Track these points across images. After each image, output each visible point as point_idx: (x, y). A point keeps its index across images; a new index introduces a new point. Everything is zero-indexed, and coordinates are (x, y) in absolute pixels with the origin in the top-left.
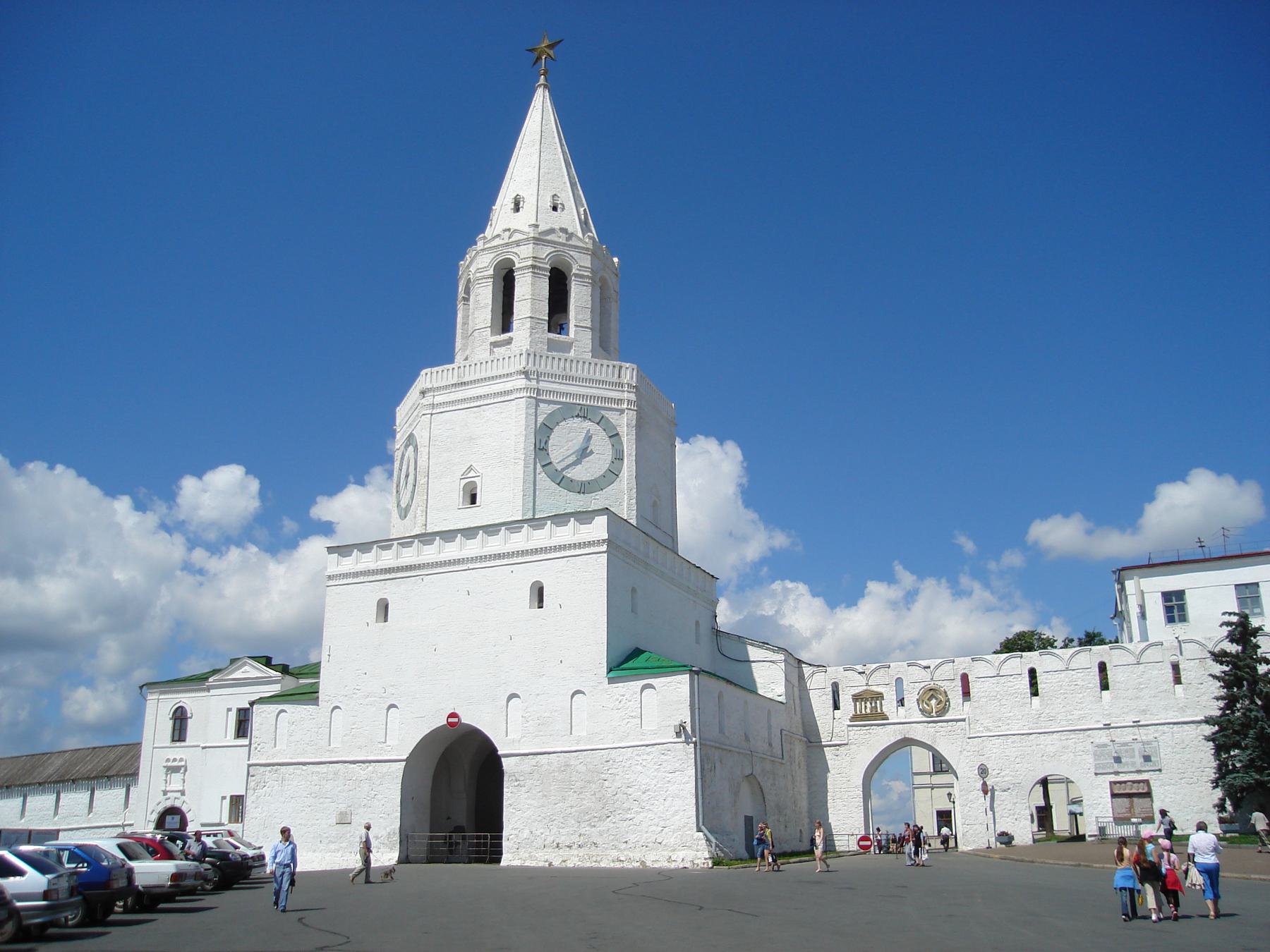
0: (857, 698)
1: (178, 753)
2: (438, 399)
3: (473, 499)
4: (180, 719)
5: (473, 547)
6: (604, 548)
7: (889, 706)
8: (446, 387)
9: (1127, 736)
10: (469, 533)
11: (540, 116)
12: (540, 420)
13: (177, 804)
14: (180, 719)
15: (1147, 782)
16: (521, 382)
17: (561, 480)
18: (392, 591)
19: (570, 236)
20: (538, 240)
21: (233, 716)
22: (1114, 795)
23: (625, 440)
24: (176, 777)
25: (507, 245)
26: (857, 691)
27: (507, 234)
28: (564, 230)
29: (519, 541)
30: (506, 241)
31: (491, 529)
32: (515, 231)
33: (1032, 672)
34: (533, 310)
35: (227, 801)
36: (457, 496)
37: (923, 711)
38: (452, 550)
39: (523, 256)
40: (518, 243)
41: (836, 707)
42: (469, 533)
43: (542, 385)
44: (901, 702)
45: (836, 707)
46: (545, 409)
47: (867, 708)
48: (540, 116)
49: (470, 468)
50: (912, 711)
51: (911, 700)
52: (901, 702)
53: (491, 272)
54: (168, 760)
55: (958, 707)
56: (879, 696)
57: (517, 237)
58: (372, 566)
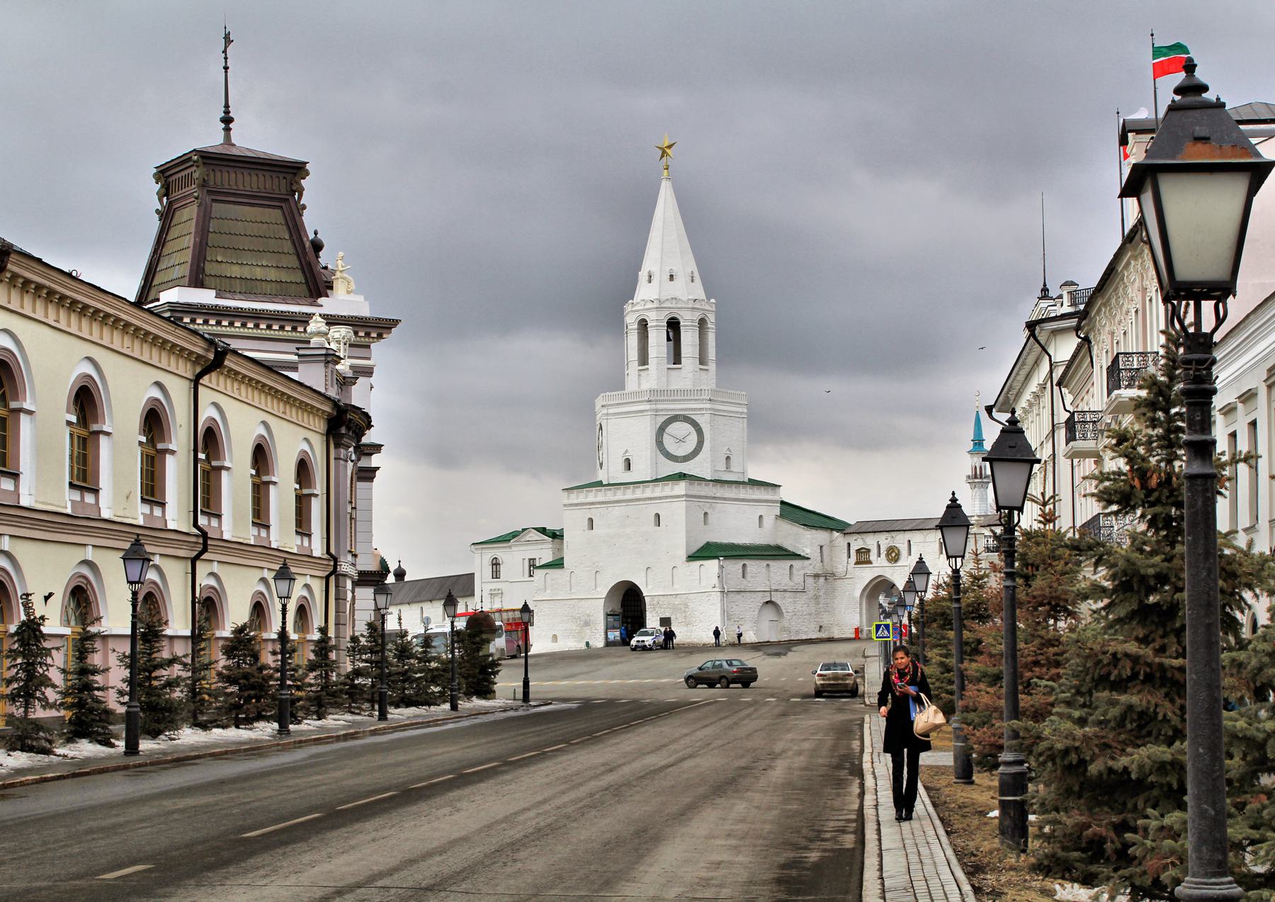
0: (858, 551)
1: (496, 585)
2: (611, 411)
4: (496, 564)
5: (629, 494)
7: (873, 556)
14: (496, 564)
17: (669, 456)
18: (595, 513)
24: (497, 599)
29: (648, 492)
36: (621, 465)
38: (620, 495)
39: (652, 317)
43: (660, 406)
45: (849, 557)
46: (661, 420)
51: (883, 556)
56: (869, 551)
57: (649, 305)
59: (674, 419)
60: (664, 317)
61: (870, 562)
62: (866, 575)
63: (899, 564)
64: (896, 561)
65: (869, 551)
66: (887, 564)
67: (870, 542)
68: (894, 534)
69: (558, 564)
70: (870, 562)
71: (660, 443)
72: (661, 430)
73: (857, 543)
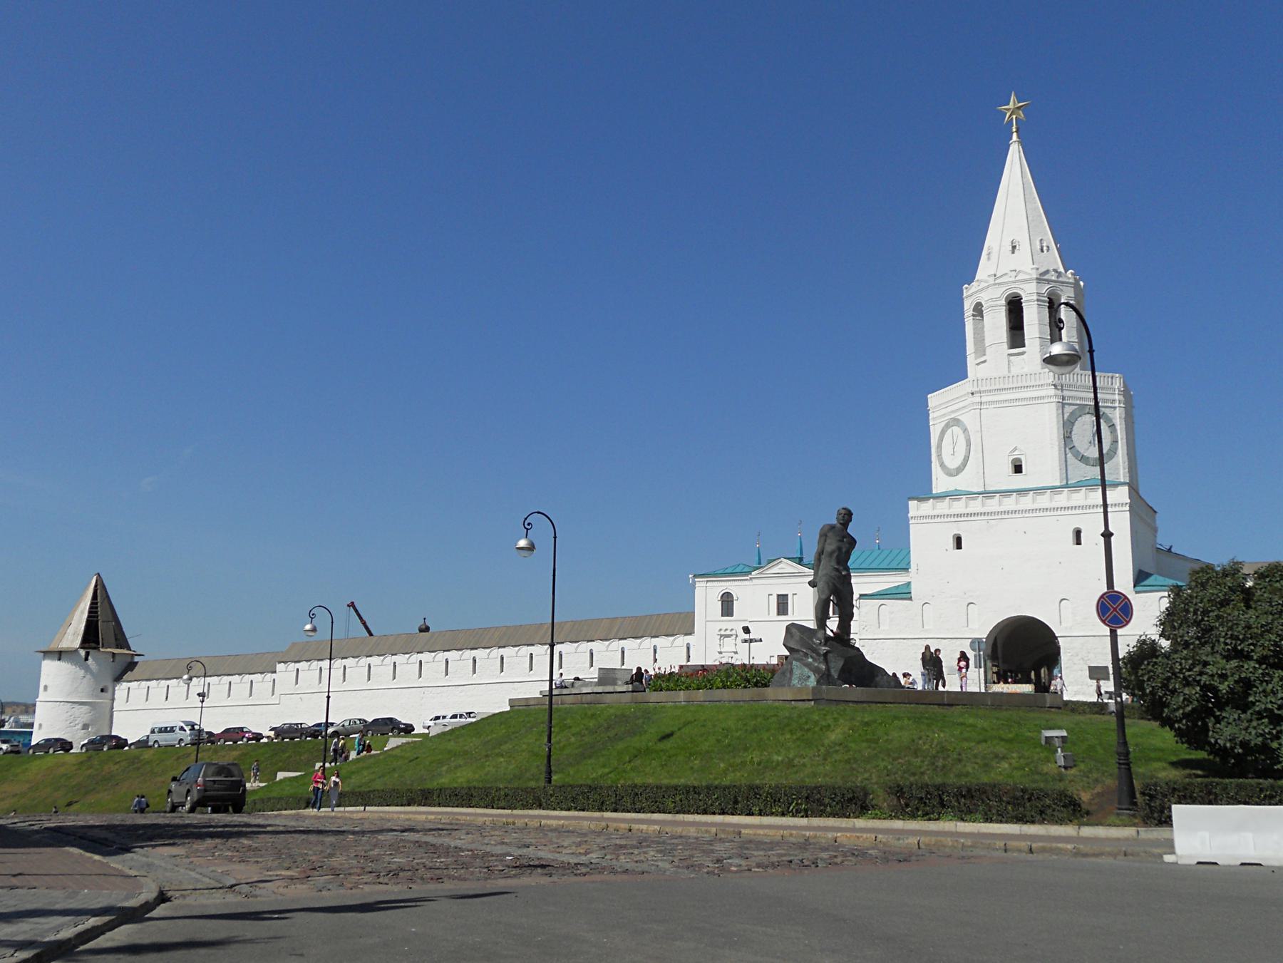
2: (984, 399)
3: (1018, 469)
6: (1127, 508)
10: (1022, 492)
11: (1015, 173)
12: (1066, 416)
16: (1052, 391)
19: (1059, 274)
20: (1039, 280)
21: (774, 600)
23: (1118, 428)
28: (1055, 271)
31: (1039, 490)
34: (1040, 332)
38: (1010, 503)
42: (1022, 492)
43: (1066, 393)
46: (1068, 410)
48: (1015, 173)
49: (1015, 449)
53: (1003, 302)
57: (1021, 277)
58: (946, 512)
69: (903, 593)
71: (1067, 437)
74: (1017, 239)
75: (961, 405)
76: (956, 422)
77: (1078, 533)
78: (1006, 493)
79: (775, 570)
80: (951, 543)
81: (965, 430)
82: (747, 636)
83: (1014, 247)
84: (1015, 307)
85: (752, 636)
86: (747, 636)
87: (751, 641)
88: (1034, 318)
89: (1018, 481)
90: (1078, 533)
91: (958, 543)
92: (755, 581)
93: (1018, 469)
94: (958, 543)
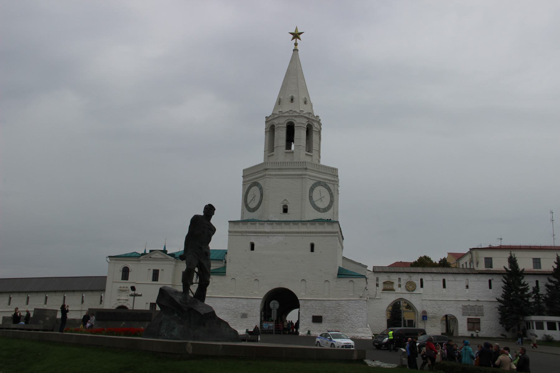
0: (384, 283)
3: (285, 210)
5: (286, 228)
7: (395, 287)
8: (276, 169)
9: (472, 304)
13: (125, 305)
15: (479, 319)
22: (468, 322)
25: (292, 116)
26: (385, 281)
27: (291, 112)
30: (291, 115)
32: (295, 112)
33: (444, 280)
35: (149, 305)
37: (407, 290)
40: (296, 116)
41: (377, 285)
42: (287, 222)
44: (400, 286)
46: (312, 182)
47: (388, 287)
49: (285, 200)
50: (403, 290)
51: (403, 287)
52: (400, 286)
53: (285, 125)
54: (120, 287)
55: (419, 290)
56: (392, 283)
59: (318, 184)
60: (305, 122)
61: (393, 290)
62: (390, 298)
63: (414, 292)
64: (413, 291)
65: (392, 283)
66: (405, 291)
67: (394, 278)
68: (411, 275)
70: (393, 290)
71: (311, 197)
72: (312, 190)
73: (383, 278)
74: (294, 96)
75: (260, 175)
76: (256, 184)
77: (312, 246)
78: (279, 222)
79: (153, 256)
80: (249, 246)
81: (261, 189)
82: (133, 292)
83: (292, 100)
84: (290, 130)
85: (136, 292)
86: (133, 292)
87: (135, 295)
88: (300, 135)
89: (285, 217)
90: (312, 246)
91: (252, 247)
92: (141, 262)
93: (285, 210)
94: (252, 247)
